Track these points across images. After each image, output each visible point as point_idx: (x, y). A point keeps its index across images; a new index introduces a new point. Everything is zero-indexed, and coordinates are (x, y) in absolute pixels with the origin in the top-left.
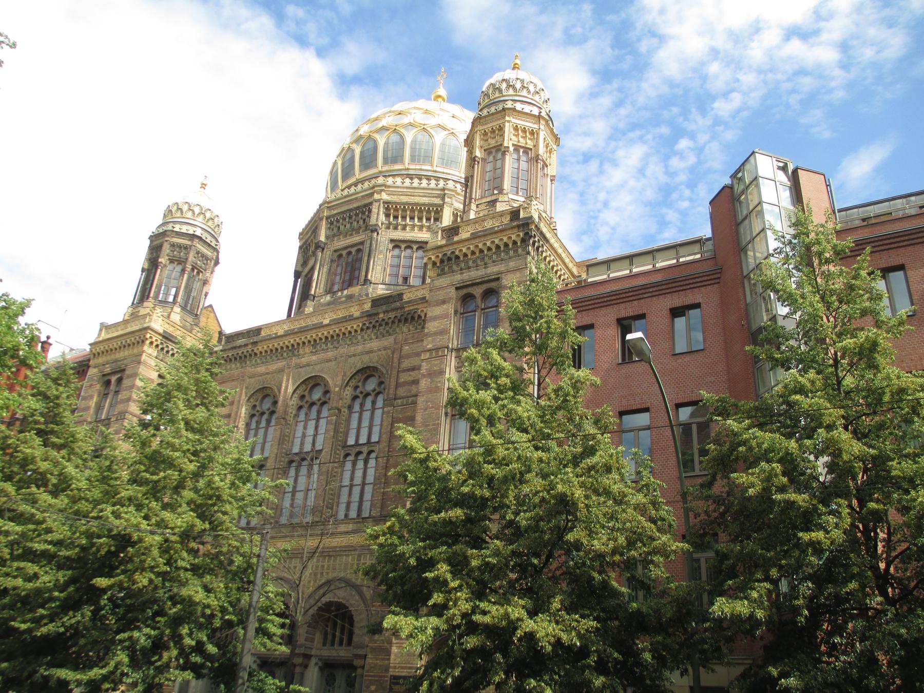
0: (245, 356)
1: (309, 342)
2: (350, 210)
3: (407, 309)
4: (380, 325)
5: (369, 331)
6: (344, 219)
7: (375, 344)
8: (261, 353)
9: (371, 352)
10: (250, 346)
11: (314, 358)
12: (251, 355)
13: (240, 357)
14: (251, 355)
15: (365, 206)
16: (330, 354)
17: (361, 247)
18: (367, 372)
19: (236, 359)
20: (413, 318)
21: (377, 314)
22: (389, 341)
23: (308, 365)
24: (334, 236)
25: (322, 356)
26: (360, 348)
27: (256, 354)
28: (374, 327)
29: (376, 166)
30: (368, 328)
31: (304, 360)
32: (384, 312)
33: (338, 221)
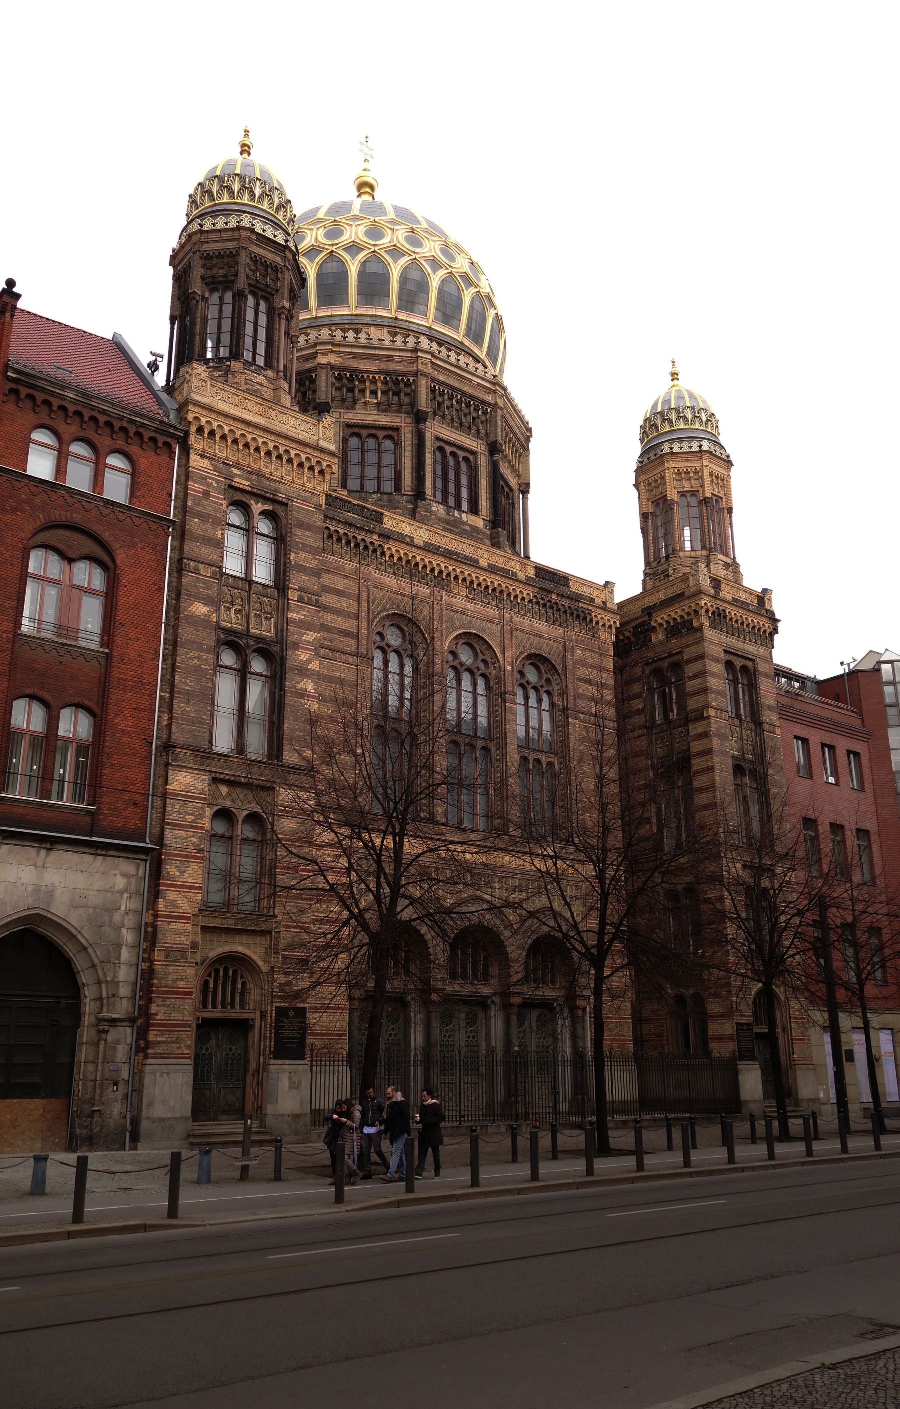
0: (366, 548)
1: (464, 580)
2: (464, 394)
3: (581, 605)
4: (552, 608)
5: (536, 608)
6: (451, 398)
7: (542, 627)
8: (392, 556)
9: (541, 637)
10: (376, 537)
11: (470, 606)
12: (375, 551)
13: (357, 545)
14: (375, 551)
15: (484, 402)
16: (492, 612)
17: (472, 458)
18: (537, 660)
19: (348, 543)
20: (585, 619)
21: (551, 592)
22: (558, 632)
23: (463, 613)
24: (435, 414)
25: (479, 608)
26: (527, 623)
27: (383, 554)
28: (545, 606)
29: (457, 329)
30: (538, 603)
31: (460, 602)
32: (558, 595)
33: (442, 394)
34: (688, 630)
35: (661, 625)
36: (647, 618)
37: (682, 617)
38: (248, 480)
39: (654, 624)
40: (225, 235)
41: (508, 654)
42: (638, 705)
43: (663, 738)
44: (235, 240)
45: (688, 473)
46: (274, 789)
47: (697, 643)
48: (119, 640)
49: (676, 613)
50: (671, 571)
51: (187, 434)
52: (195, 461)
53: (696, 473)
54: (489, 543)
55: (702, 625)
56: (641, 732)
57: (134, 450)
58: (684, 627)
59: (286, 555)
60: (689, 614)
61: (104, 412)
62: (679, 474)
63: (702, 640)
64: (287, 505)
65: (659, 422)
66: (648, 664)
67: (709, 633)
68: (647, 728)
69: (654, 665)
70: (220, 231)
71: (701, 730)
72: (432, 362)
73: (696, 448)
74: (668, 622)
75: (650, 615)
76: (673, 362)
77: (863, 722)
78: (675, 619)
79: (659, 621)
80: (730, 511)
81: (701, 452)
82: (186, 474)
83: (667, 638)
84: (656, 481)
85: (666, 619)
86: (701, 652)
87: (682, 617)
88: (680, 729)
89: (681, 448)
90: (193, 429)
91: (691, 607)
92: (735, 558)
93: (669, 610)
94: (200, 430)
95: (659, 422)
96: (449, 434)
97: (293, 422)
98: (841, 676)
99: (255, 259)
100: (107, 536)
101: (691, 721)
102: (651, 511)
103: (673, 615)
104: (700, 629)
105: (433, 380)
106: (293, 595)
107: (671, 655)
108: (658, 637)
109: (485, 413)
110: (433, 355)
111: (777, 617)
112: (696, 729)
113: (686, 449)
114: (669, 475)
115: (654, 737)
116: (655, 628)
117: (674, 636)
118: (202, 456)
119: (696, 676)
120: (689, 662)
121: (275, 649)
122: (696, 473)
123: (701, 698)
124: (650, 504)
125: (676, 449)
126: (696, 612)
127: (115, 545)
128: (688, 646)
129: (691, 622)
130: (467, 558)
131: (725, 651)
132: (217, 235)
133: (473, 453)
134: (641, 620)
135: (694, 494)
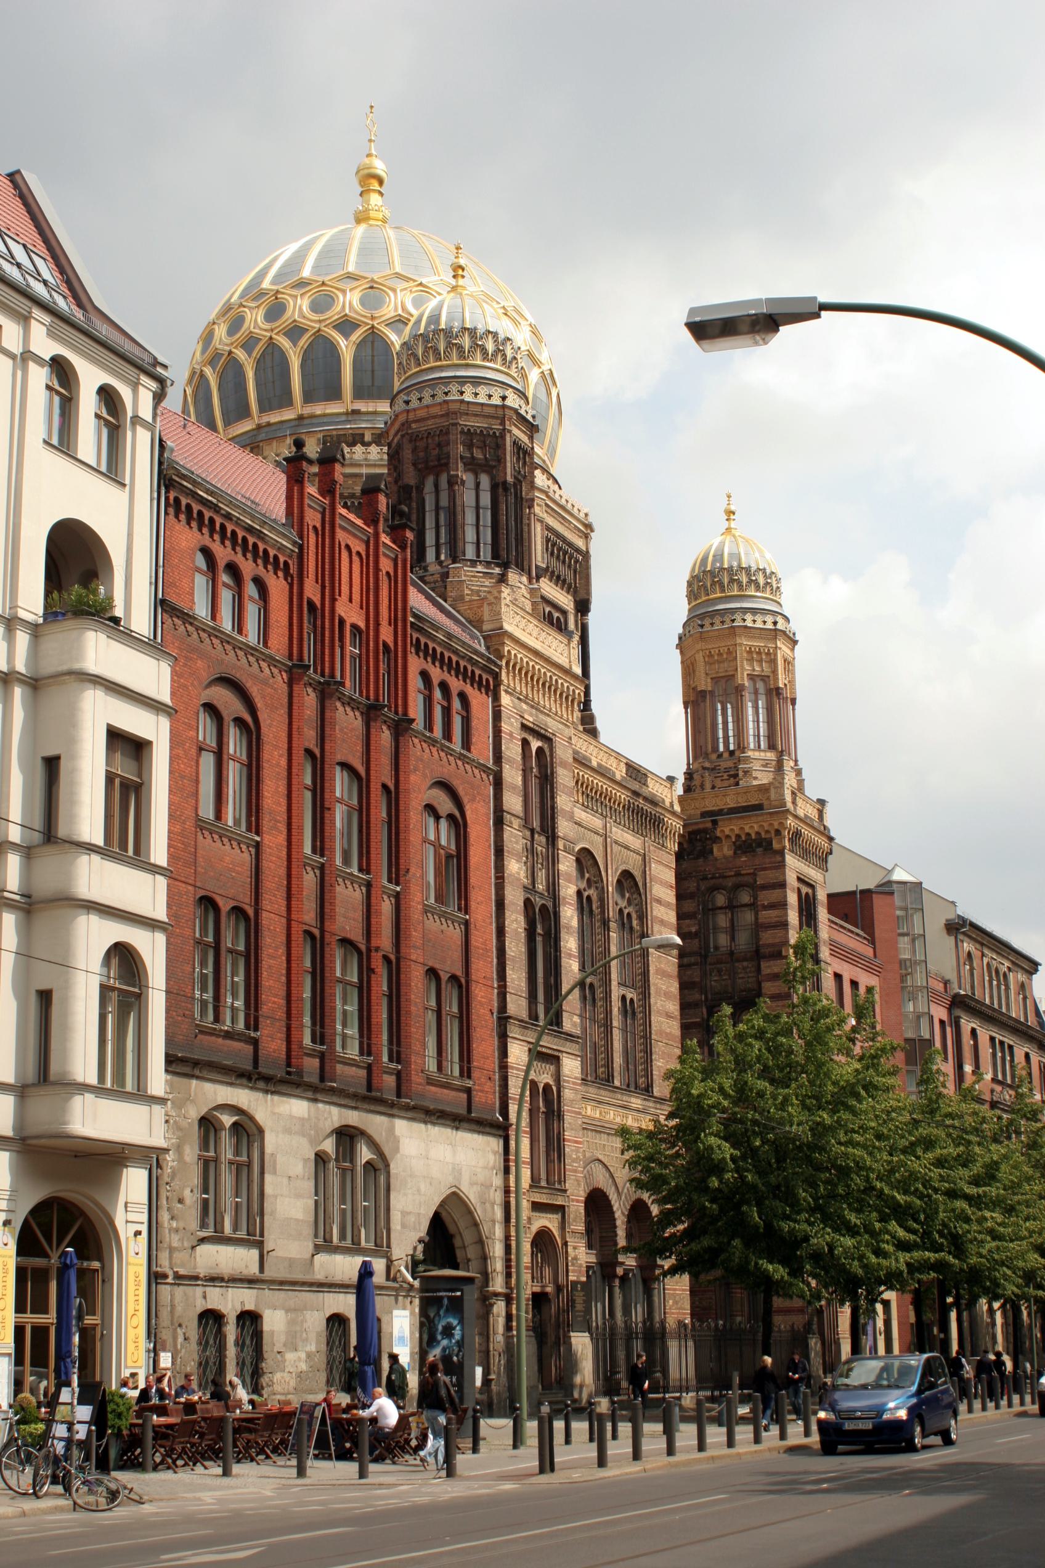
2: (564, 540)
16: (597, 822)
34: (765, 850)
35: (728, 837)
36: (709, 825)
37: (758, 833)
38: (531, 715)
39: (718, 834)
40: (487, 410)
41: (610, 871)
42: (689, 926)
43: (719, 971)
44: (497, 418)
45: (759, 653)
46: (558, 1058)
47: (776, 868)
48: (473, 905)
49: (751, 826)
50: (741, 774)
51: (500, 667)
52: (505, 700)
53: (768, 654)
54: (581, 728)
55: (784, 848)
56: (693, 960)
57: (469, 689)
58: (760, 845)
59: (553, 798)
60: (767, 832)
61: (456, 652)
62: (750, 652)
63: (782, 865)
64: (548, 740)
65: (726, 581)
66: (705, 878)
67: (791, 860)
68: (701, 955)
69: (712, 882)
70: (482, 405)
71: (776, 970)
72: (547, 505)
73: (770, 626)
74: (738, 836)
75: (715, 823)
76: (729, 497)
77: (874, 949)
78: (748, 834)
79: (727, 832)
80: (793, 701)
81: (776, 630)
82: (497, 716)
83: (735, 853)
84: (720, 654)
85: (737, 832)
86: (781, 879)
87: (758, 833)
88: (745, 964)
89: (754, 621)
90: (504, 663)
91: (771, 825)
92: (796, 761)
93: (740, 822)
94: (508, 663)
95: (726, 581)
96: (548, 589)
97: (555, 643)
98: (853, 893)
99: (516, 443)
100: (461, 791)
101: (764, 957)
102: (710, 689)
103: (747, 830)
104: (781, 853)
105: (549, 528)
106: (561, 844)
107: (738, 874)
108: (723, 851)
109: (577, 561)
110: (548, 496)
111: (832, 834)
112: (769, 967)
113: (759, 625)
114: (741, 653)
115: (708, 967)
116: (719, 838)
117: (745, 853)
118: (506, 691)
119: (772, 906)
120: (764, 887)
121: (550, 905)
122: (768, 654)
123: (779, 933)
124: (709, 680)
125: (749, 623)
126: (778, 832)
127: (465, 800)
128: (765, 869)
129: (770, 843)
130: (585, 757)
131: (799, 879)
132: (479, 409)
133: (564, 613)
134: (701, 826)
135: (764, 678)
